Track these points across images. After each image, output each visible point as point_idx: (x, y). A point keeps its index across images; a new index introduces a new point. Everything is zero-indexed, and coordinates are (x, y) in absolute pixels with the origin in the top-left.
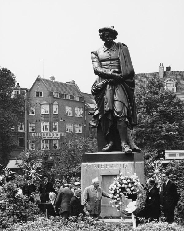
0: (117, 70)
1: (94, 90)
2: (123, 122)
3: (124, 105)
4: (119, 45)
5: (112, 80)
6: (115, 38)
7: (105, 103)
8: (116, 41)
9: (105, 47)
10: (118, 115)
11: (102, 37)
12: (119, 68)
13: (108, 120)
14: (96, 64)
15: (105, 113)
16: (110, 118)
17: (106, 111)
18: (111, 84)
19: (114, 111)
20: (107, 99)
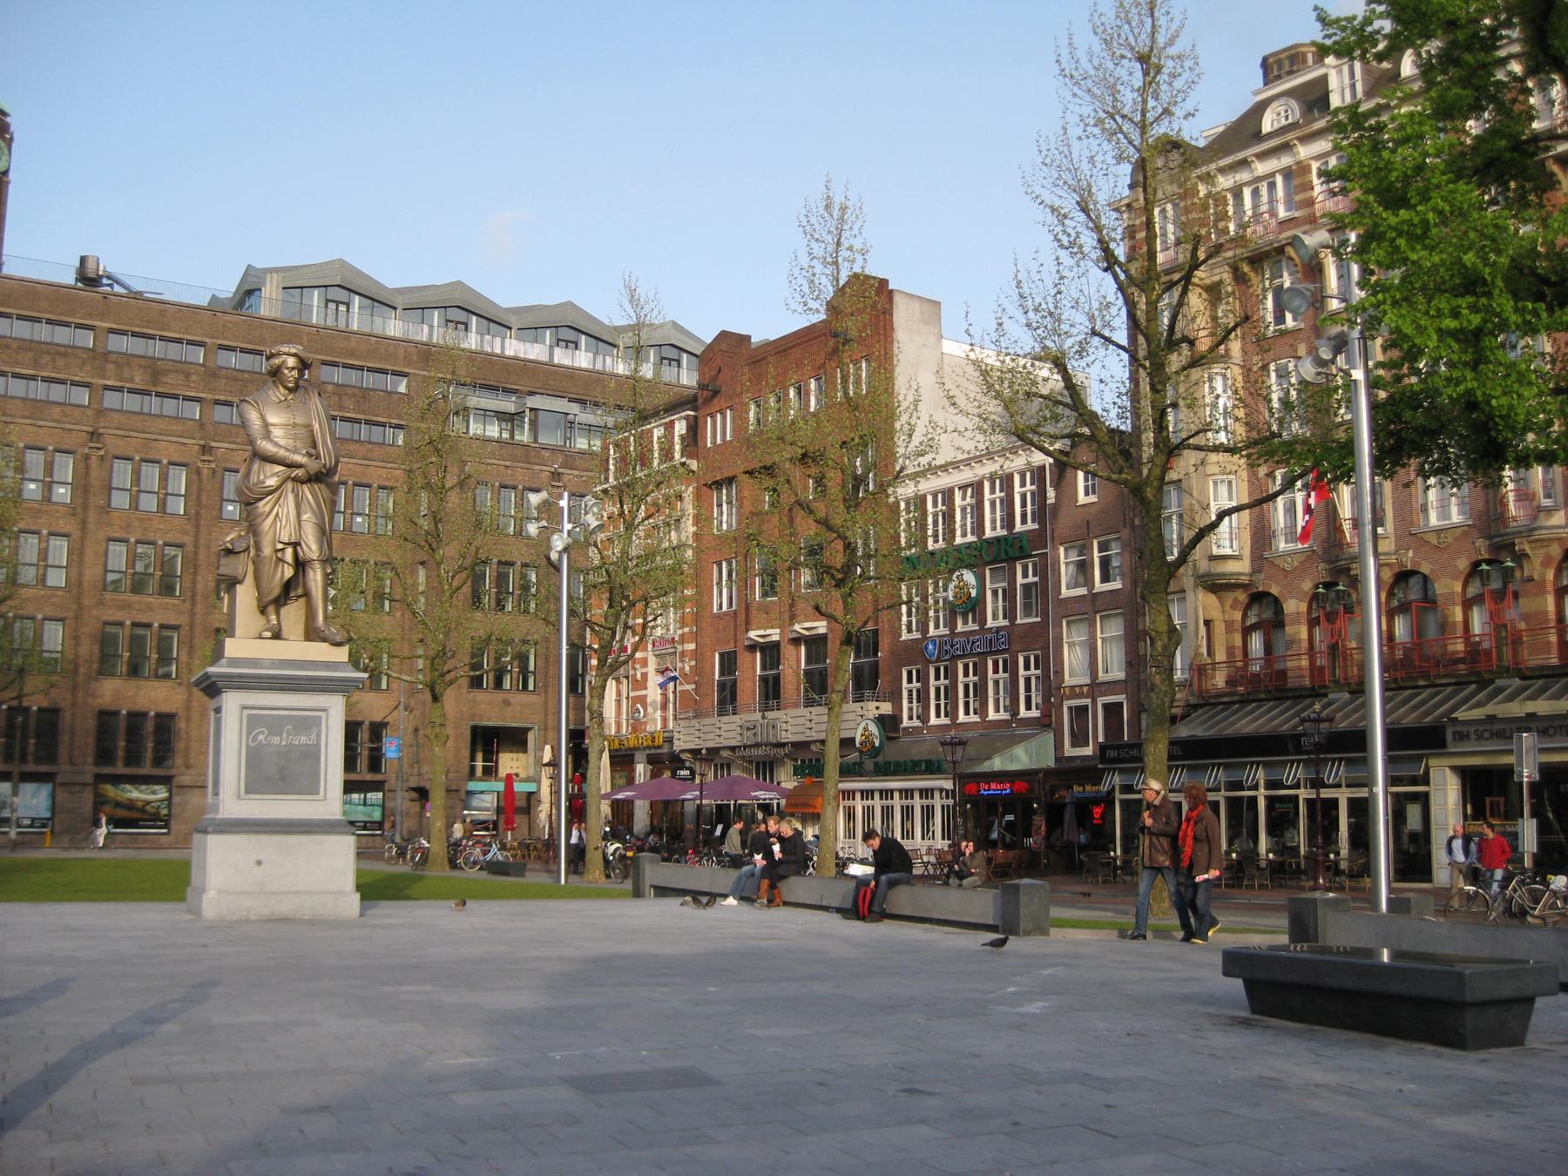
0: (313, 451)
15: (280, 546)
18: (294, 479)
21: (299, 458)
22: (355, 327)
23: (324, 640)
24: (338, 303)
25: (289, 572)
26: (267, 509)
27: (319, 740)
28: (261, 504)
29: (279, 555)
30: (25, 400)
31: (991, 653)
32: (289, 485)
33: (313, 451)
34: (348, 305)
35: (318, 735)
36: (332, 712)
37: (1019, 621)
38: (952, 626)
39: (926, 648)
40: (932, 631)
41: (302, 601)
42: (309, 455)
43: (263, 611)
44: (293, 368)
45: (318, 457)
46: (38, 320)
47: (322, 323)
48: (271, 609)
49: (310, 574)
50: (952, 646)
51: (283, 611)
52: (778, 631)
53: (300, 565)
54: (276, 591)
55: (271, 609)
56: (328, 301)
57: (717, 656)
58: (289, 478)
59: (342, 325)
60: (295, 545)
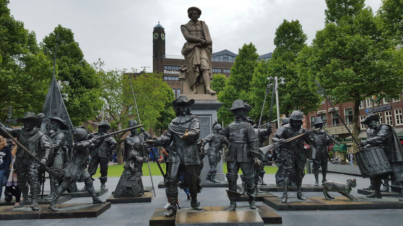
0: (203, 37)
1: (184, 51)
2: (208, 73)
3: (208, 62)
4: (201, 22)
5: (199, 44)
6: (199, 17)
7: (195, 60)
8: (199, 19)
9: (191, 22)
10: (204, 67)
11: (190, 16)
12: (204, 36)
13: (195, 71)
14: (187, 33)
15: (194, 67)
16: (198, 70)
17: (195, 65)
18: (198, 47)
19: (201, 65)
20: (196, 57)
21: (198, 38)
22: (230, 62)
23: (209, 93)
24: (226, 58)
25: (198, 75)
26: (190, 56)
27: (209, 124)
28: (188, 55)
29: (195, 70)
30: (171, 80)
31: (385, 110)
32: (197, 48)
33: (203, 37)
34: (228, 58)
35: (209, 123)
36: (213, 116)
37: (393, 102)
38: (373, 105)
39: (366, 111)
40: (367, 107)
41: (203, 85)
42: (202, 38)
43: (192, 88)
44: (195, 14)
45: (205, 39)
46: (173, 66)
47: (223, 62)
48: (194, 87)
49: (204, 75)
50: (374, 110)
51: (198, 87)
52: (325, 110)
53: (202, 72)
54: (195, 81)
55: (194, 87)
56: (224, 58)
57: (310, 117)
58: (196, 46)
59: (227, 62)
60: (199, 66)
